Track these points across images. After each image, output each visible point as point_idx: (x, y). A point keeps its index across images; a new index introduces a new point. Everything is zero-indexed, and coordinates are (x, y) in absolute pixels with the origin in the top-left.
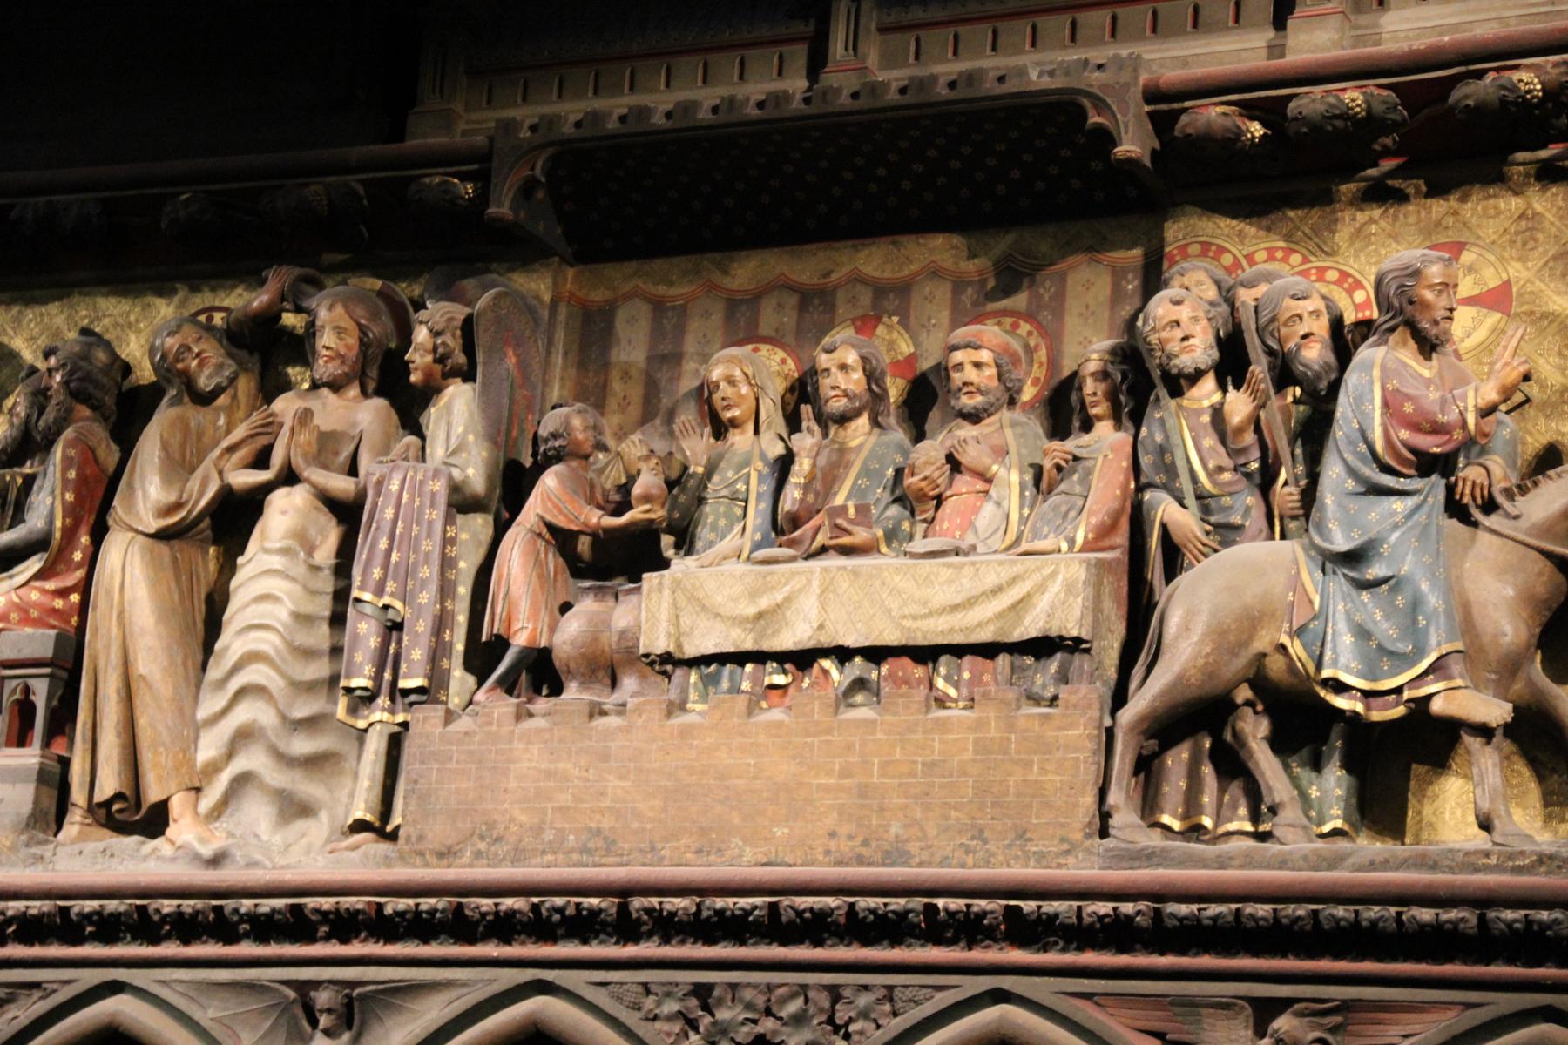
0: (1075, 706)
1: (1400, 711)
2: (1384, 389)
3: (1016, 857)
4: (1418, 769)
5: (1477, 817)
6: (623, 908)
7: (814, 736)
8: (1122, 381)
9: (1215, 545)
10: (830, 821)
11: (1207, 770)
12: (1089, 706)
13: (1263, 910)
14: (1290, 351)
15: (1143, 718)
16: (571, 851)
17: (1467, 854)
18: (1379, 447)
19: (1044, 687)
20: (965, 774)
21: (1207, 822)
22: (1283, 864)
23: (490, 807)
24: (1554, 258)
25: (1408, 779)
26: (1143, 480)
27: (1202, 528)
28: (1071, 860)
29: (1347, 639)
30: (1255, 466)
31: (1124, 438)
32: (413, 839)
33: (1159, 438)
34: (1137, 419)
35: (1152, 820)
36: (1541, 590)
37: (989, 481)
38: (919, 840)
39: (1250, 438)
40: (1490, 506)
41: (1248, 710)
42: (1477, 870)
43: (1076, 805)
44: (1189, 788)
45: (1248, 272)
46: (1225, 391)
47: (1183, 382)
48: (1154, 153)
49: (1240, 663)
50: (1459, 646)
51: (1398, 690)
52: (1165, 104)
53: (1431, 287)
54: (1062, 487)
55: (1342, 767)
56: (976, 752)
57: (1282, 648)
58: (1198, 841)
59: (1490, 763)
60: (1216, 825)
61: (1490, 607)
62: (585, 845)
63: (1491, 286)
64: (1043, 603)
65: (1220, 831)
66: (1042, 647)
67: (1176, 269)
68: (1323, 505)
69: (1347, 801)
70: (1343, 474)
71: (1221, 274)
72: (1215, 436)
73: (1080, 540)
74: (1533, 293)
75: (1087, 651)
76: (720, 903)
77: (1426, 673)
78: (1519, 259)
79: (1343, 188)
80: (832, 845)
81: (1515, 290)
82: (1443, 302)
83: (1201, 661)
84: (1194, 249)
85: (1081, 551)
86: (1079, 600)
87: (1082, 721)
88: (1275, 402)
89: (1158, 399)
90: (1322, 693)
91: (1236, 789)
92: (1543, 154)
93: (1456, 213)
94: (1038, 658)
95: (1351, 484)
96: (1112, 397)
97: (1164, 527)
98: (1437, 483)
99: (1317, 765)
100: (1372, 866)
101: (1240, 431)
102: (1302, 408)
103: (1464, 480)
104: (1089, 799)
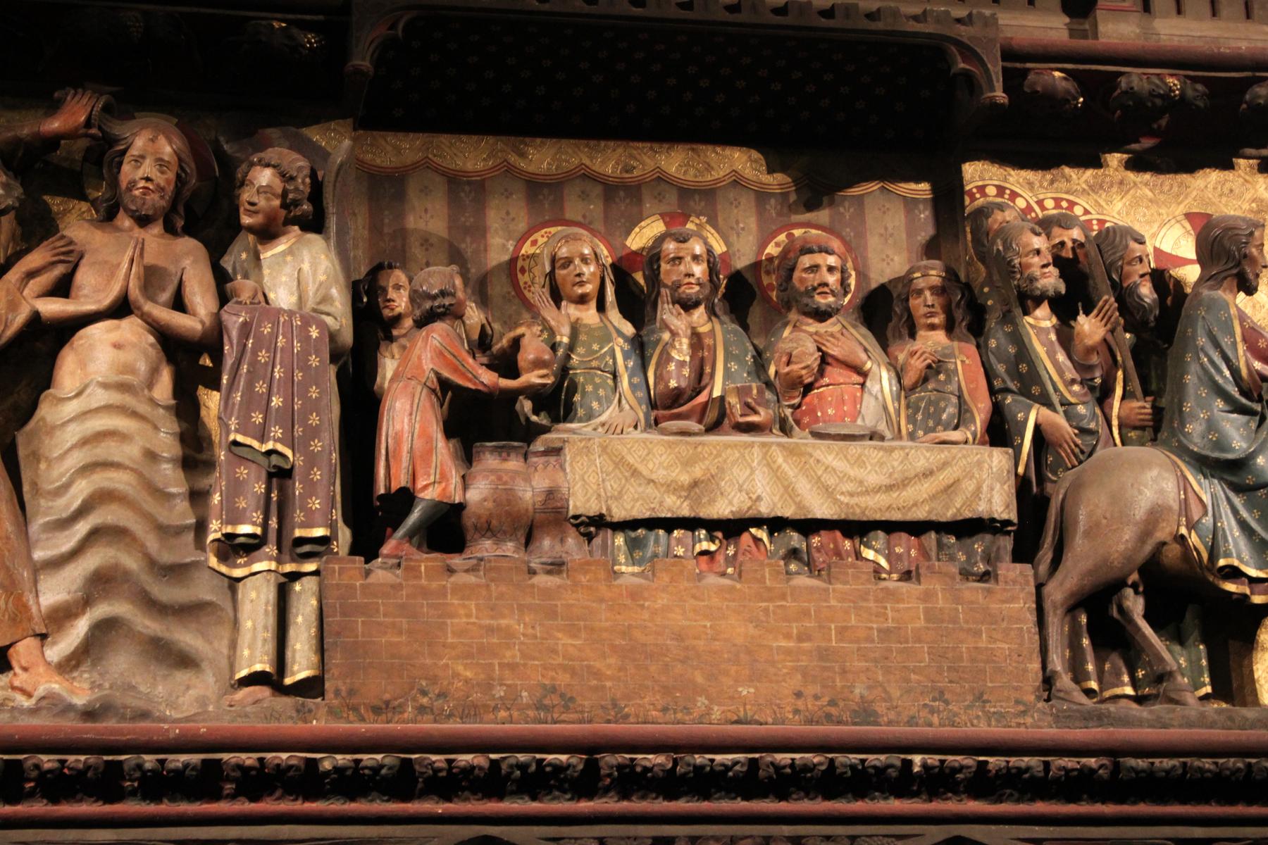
6: (592, 767)
7: (770, 600)
10: (796, 682)
13: (1207, 763)
16: (528, 707)
20: (920, 641)
23: (428, 661)
30: (1098, 381)
32: (344, 694)
37: (865, 375)
38: (885, 701)
56: (928, 620)
60: (1102, 690)
62: (540, 701)
65: (1107, 694)
76: (699, 759)
80: (800, 704)
87: (1022, 595)
101: (1090, 350)
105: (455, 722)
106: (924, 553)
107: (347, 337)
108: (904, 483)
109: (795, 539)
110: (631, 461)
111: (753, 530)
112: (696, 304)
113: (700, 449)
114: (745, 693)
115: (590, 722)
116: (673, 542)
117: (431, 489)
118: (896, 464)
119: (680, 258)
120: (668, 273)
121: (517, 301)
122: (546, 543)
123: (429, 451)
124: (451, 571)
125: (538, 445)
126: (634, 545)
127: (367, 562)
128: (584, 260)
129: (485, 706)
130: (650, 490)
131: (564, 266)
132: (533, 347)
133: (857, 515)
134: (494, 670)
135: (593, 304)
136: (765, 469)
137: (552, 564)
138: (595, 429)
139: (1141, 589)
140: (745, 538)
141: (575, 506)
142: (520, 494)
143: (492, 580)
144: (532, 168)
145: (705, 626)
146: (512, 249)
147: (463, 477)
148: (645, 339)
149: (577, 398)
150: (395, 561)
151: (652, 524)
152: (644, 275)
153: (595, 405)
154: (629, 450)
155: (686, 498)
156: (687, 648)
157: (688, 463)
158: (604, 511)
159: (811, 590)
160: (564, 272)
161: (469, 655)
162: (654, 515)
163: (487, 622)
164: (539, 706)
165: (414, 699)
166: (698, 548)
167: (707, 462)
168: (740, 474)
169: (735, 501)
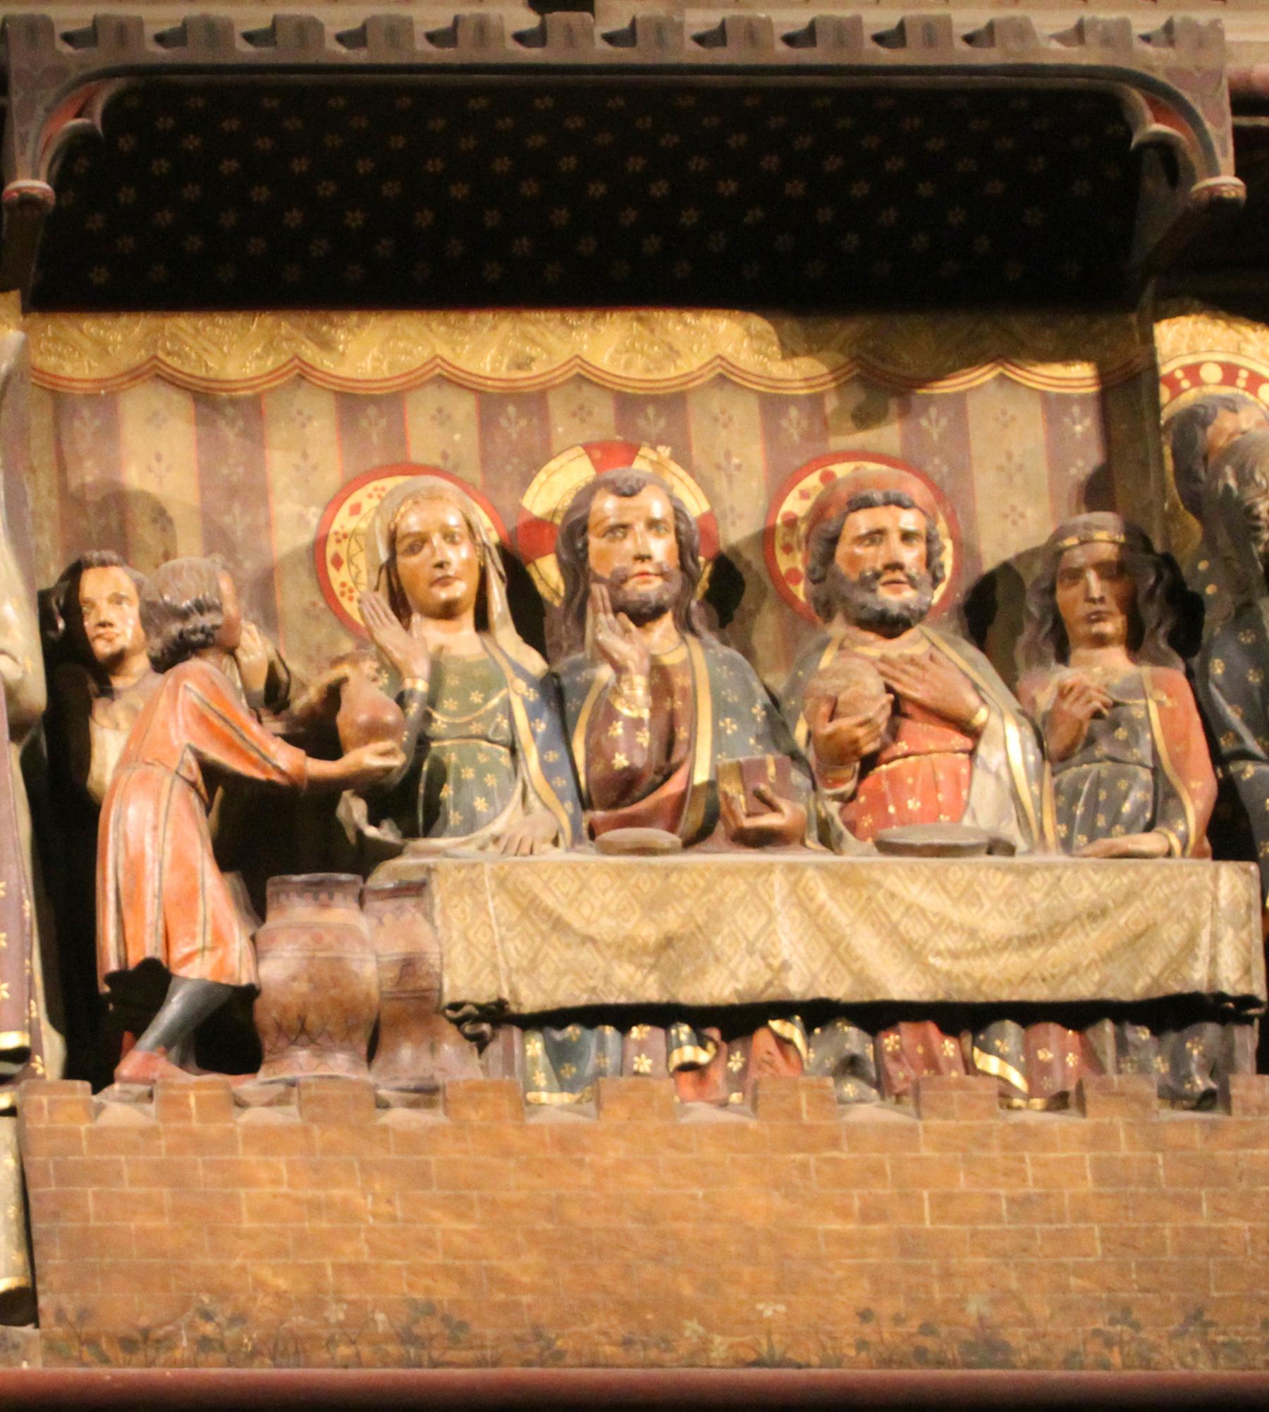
7: (812, 1149)
10: (861, 1292)
16: (387, 1338)
20: (1086, 1218)
23: (210, 1261)
32: (71, 1316)
37: (974, 734)
56: (1100, 1181)
62: (408, 1329)
80: (868, 1330)
105: (262, 1365)
106: (1092, 1059)
107: (36, 694)
108: (1051, 932)
109: (852, 1038)
110: (549, 900)
111: (775, 1025)
112: (657, 612)
113: (674, 878)
114: (768, 1313)
115: (495, 1364)
116: (632, 1049)
117: (197, 961)
118: (1037, 896)
119: (625, 527)
120: (603, 555)
121: (329, 618)
122: (406, 1053)
123: (190, 896)
124: (241, 1104)
125: (383, 877)
126: (560, 1055)
127: (96, 1090)
128: (449, 536)
129: (313, 1338)
130: (587, 955)
131: (413, 550)
132: (365, 699)
133: (966, 992)
134: (324, 1276)
135: (468, 618)
136: (796, 913)
137: (417, 1090)
138: (482, 848)
140: (762, 1039)
141: (454, 988)
142: (355, 967)
143: (313, 1119)
144: (345, 371)
145: (693, 1197)
146: (314, 522)
147: (253, 939)
148: (565, 681)
149: (447, 792)
150: (144, 1088)
151: (592, 1016)
152: (560, 560)
153: (480, 804)
154: (546, 886)
155: (653, 968)
156: (662, 1236)
157: (653, 905)
158: (506, 995)
159: (886, 1130)
160: (414, 560)
161: (280, 1251)
162: (596, 1000)
163: (310, 1193)
164: (407, 1338)
165: (191, 1326)
166: (678, 1058)
167: (688, 903)
168: (751, 924)
169: (742, 973)
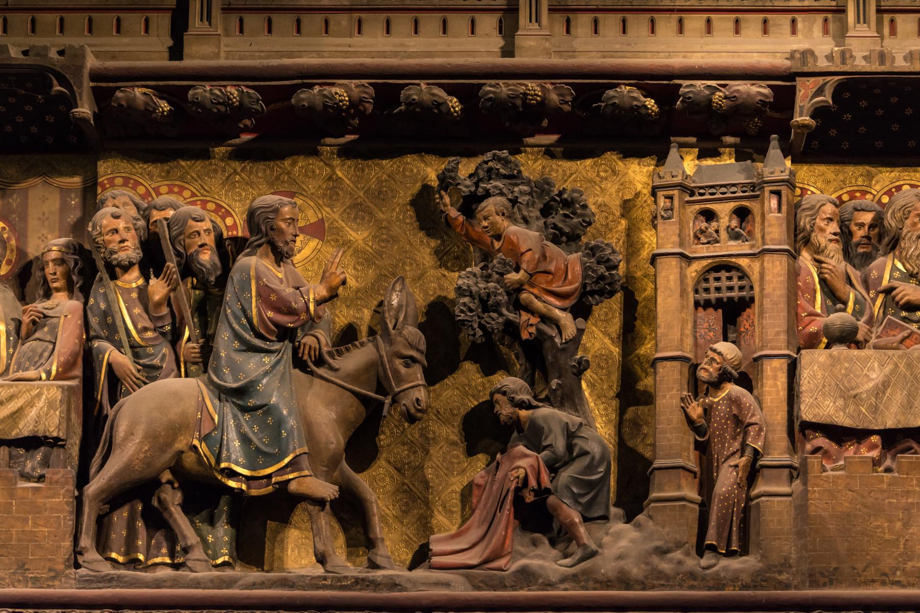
0: (57, 482)
1: (270, 489)
2: (257, 283)
3: (19, 581)
4: (271, 524)
5: (316, 555)
8: (74, 267)
9: (144, 379)
11: (140, 524)
12: (67, 483)
14: (192, 255)
15: (102, 491)
17: (313, 578)
18: (255, 320)
19: (33, 469)
21: (141, 557)
22: (197, 584)
24: (350, 207)
25: (265, 530)
26: (92, 333)
27: (135, 367)
28: (57, 583)
29: (237, 444)
30: (168, 328)
31: (75, 304)
33: (103, 306)
34: (86, 291)
35: (105, 556)
36: (351, 416)
39: (165, 310)
40: (320, 361)
41: (169, 486)
42: (318, 588)
43: (59, 547)
44: (128, 535)
45: (159, 200)
46: (147, 279)
47: (118, 270)
48: (95, 114)
49: (168, 456)
50: (306, 449)
51: (269, 477)
52: (106, 84)
53: (285, 220)
54: (37, 335)
55: (227, 523)
57: (194, 448)
58: (135, 569)
59: (323, 522)
60: (147, 559)
61: (324, 426)
63: (312, 221)
64: (33, 413)
65: (150, 563)
66: (31, 443)
67: (108, 194)
68: (219, 357)
69: (231, 544)
70: (232, 337)
71: (138, 199)
72: (141, 307)
73: (54, 373)
74: (337, 228)
75: (63, 446)
77: (286, 466)
78: (328, 206)
79: (216, 150)
81: (326, 225)
82: (291, 230)
83: (142, 456)
84: (119, 181)
85: (54, 380)
86: (58, 412)
87: (62, 491)
88: (182, 288)
89: (101, 279)
90: (216, 474)
91: (159, 536)
92: (342, 140)
93: (289, 173)
94: (27, 450)
95: (236, 344)
96: (68, 276)
97: (109, 365)
98: (287, 346)
99: (212, 522)
100: (254, 586)
101: (158, 305)
102: (197, 292)
103: (304, 345)
104: (68, 543)
139: (176, 485)
